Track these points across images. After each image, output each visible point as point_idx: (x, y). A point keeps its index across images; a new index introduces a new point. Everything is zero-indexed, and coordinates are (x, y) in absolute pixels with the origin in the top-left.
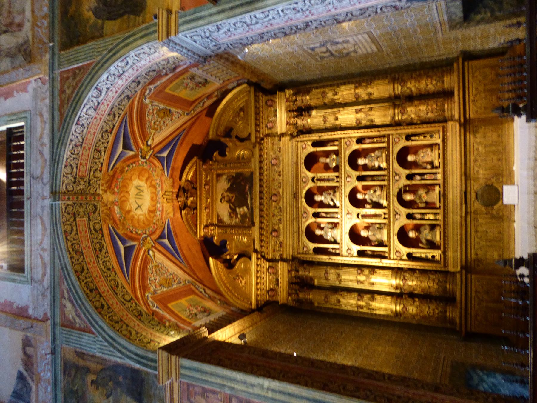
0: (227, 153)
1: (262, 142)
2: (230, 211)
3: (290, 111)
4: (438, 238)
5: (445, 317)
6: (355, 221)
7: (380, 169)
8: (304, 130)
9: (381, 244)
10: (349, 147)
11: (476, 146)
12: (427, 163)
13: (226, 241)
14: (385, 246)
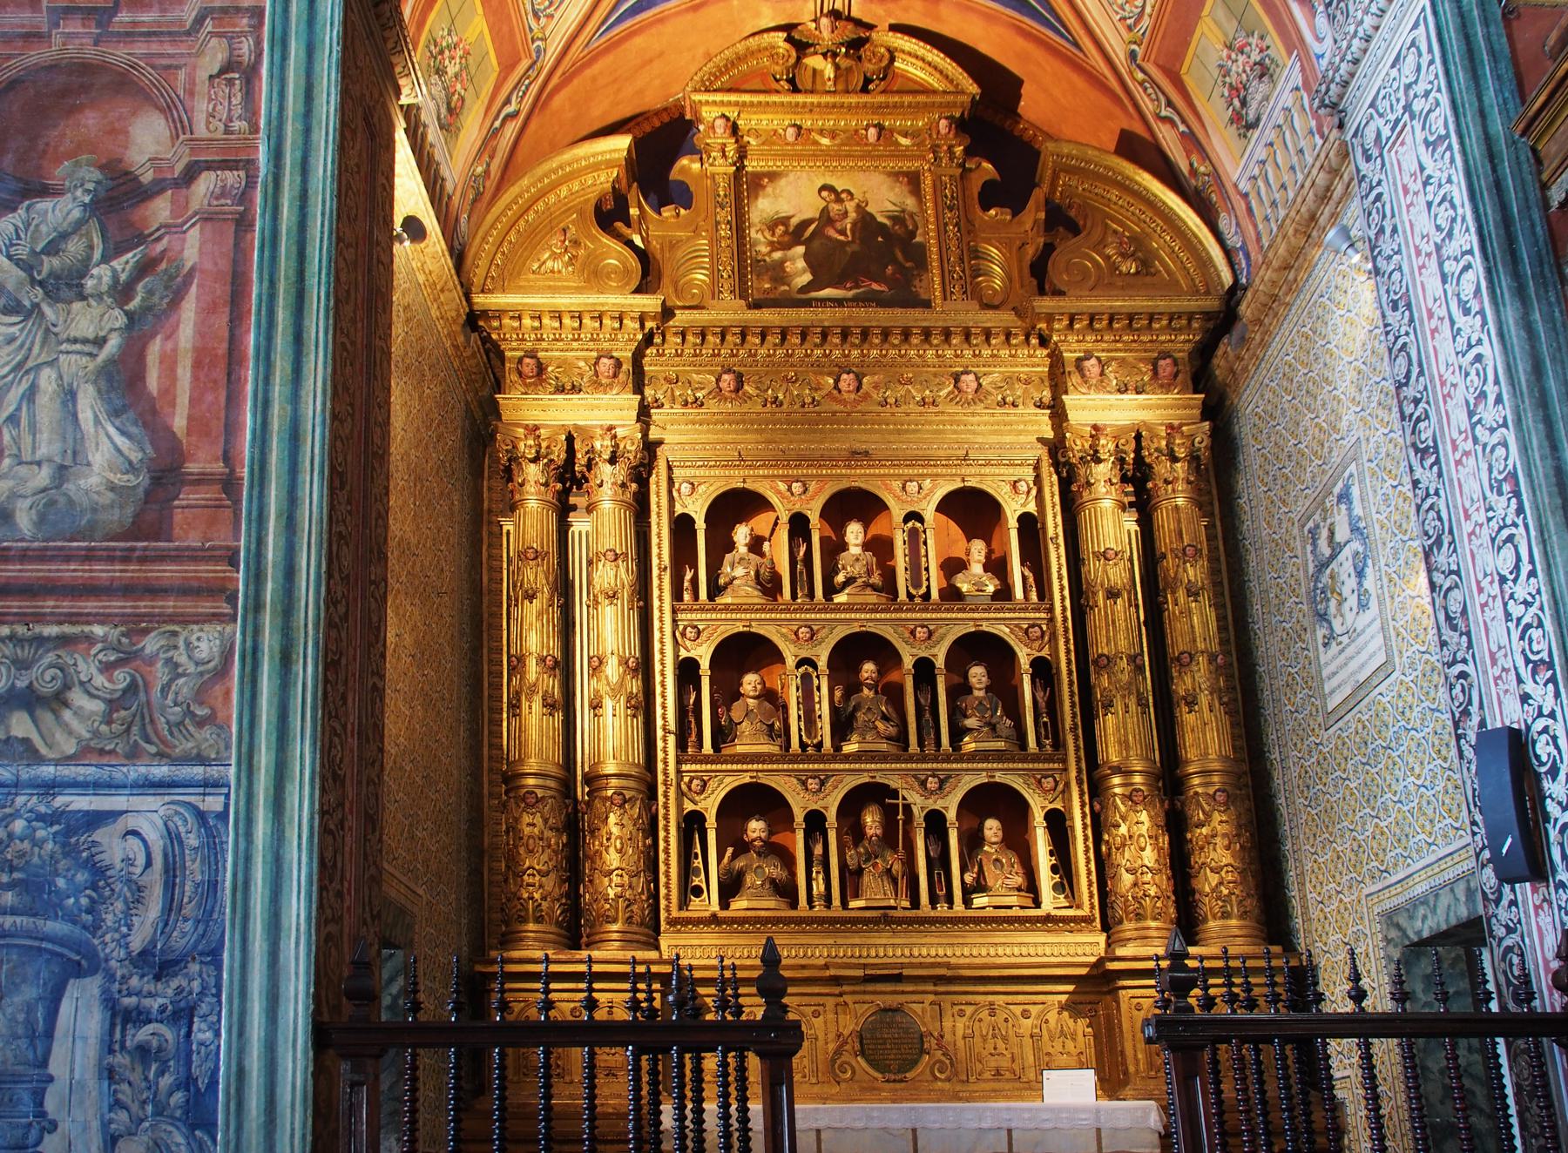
0: (992, 212)
1: (1034, 341)
2: (794, 221)
3: (1138, 437)
7: (957, 733)
8: (1074, 488)
9: (723, 734)
11: (1034, 1010)
12: (981, 871)
13: (687, 207)
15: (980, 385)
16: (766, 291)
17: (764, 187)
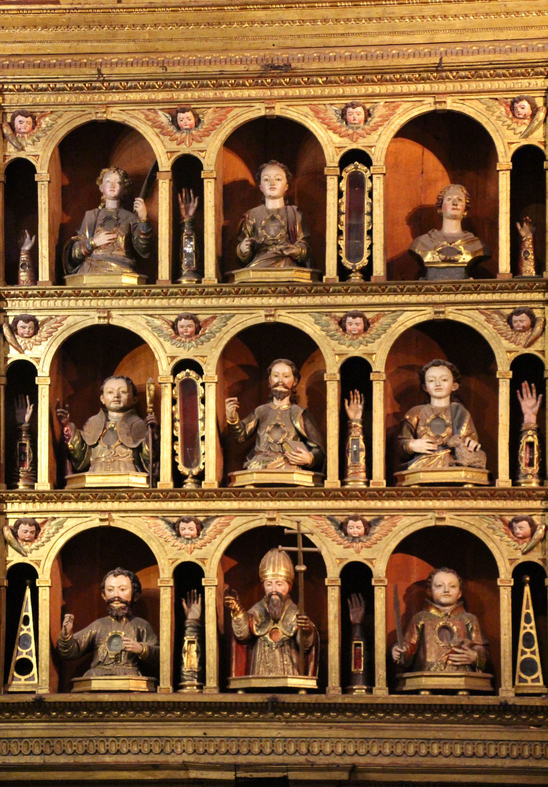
4: (96, 685)
10: (502, 323)
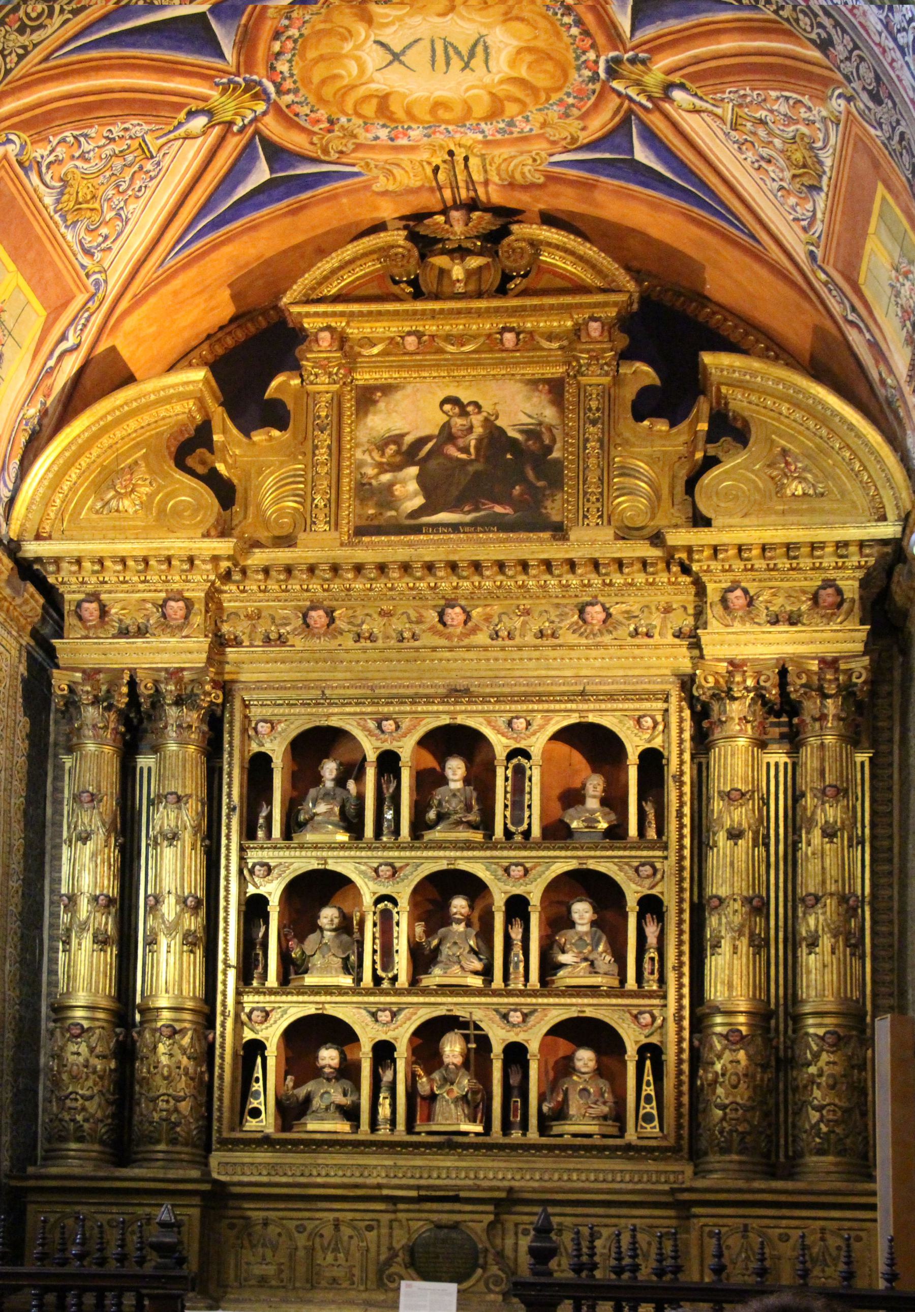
0: (646, 423)
2: (408, 440)
5: (63, 1139)
6: (368, 890)
10: (631, 872)
14: (284, 980)
15: (609, 615)
16: (370, 518)
17: (375, 402)
